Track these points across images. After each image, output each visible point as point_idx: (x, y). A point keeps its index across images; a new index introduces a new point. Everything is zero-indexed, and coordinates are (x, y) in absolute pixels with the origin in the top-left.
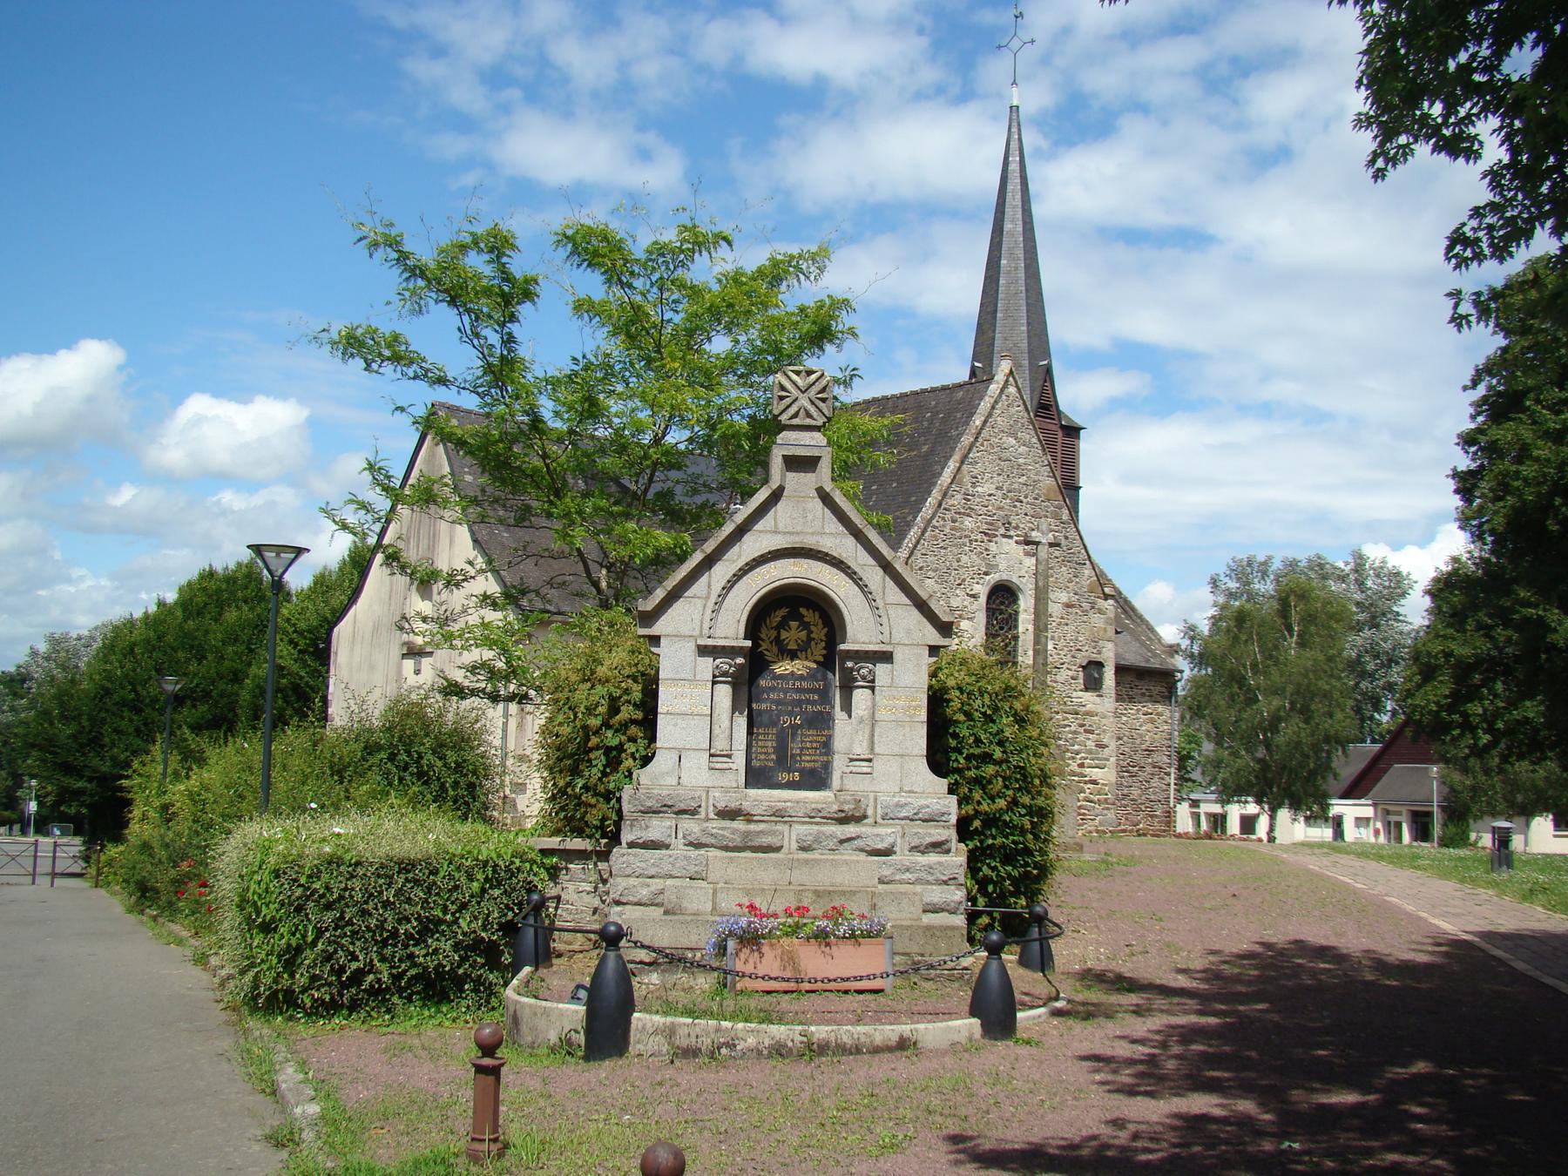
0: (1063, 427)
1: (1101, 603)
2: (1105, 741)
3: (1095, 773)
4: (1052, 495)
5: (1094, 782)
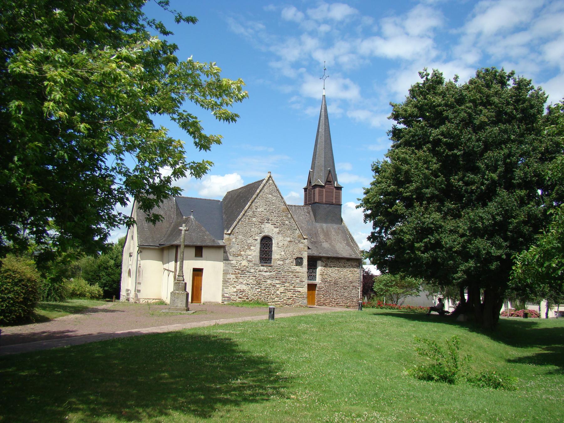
0: (335, 187)
1: (302, 241)
2: (303, 280)
3: (299, 289)
4: (285, 210)
5: (299, 292)
